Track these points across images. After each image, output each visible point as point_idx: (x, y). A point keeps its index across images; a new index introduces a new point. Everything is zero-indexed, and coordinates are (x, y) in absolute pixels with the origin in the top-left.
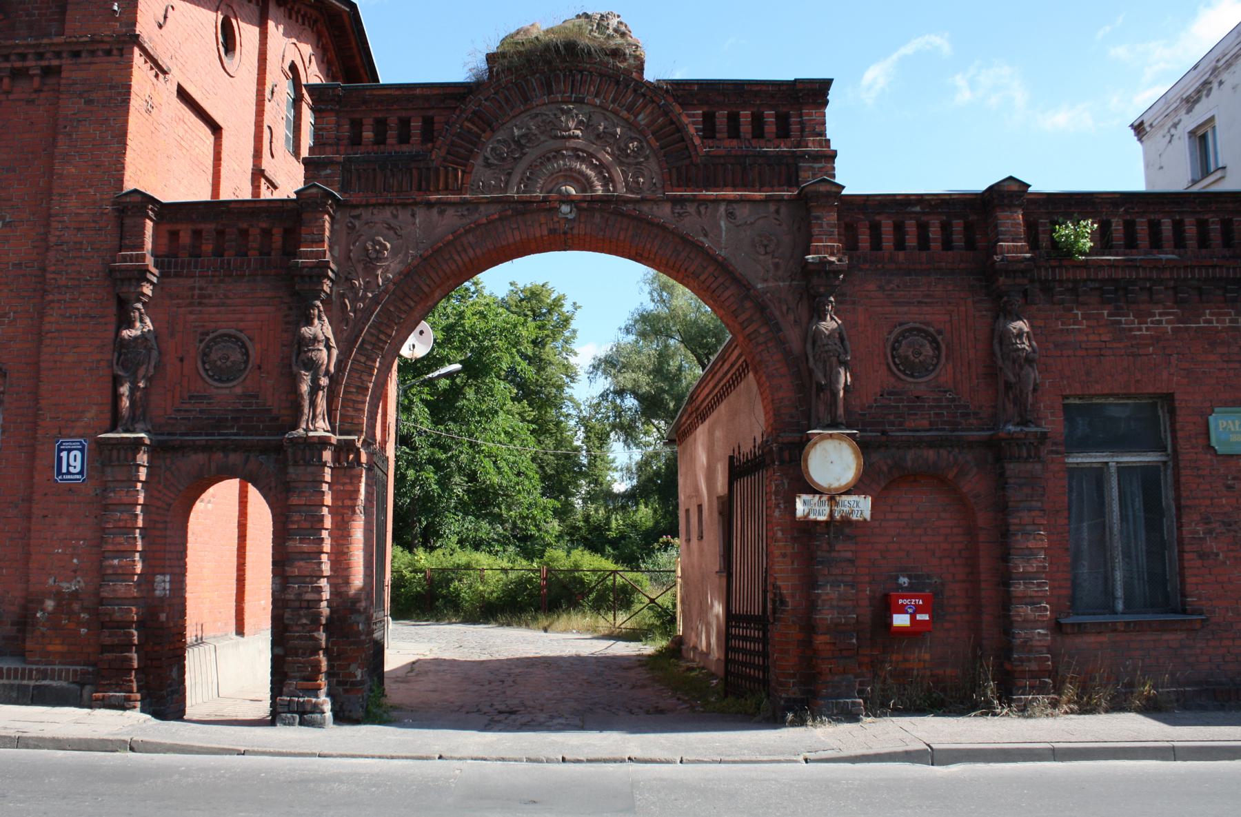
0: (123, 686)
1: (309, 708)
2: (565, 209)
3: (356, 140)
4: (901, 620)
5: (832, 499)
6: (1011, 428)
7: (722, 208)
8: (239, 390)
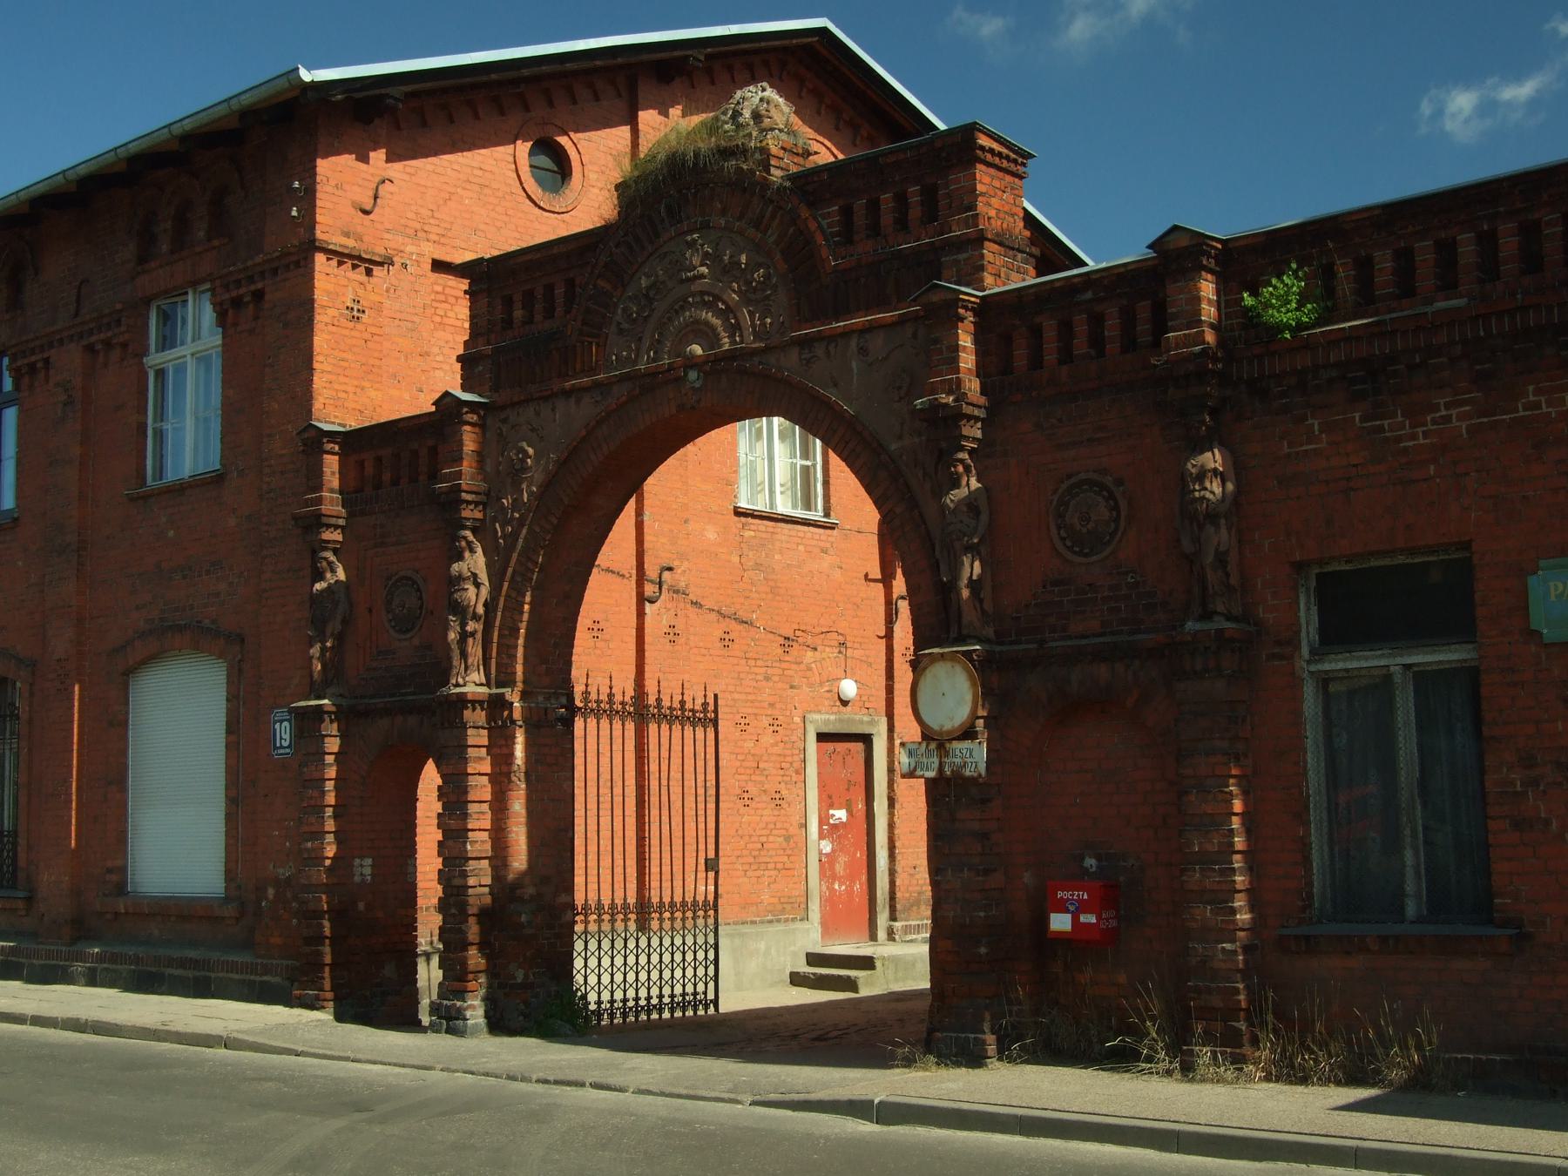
0: (316, 984)
1: (453, 1014)
2: (693, 375)
3: (508, 323)
4: (1060, 922)
5: (941, 746)
6: (1190, 625)
7: (853, 343)
8: (416, 641)
